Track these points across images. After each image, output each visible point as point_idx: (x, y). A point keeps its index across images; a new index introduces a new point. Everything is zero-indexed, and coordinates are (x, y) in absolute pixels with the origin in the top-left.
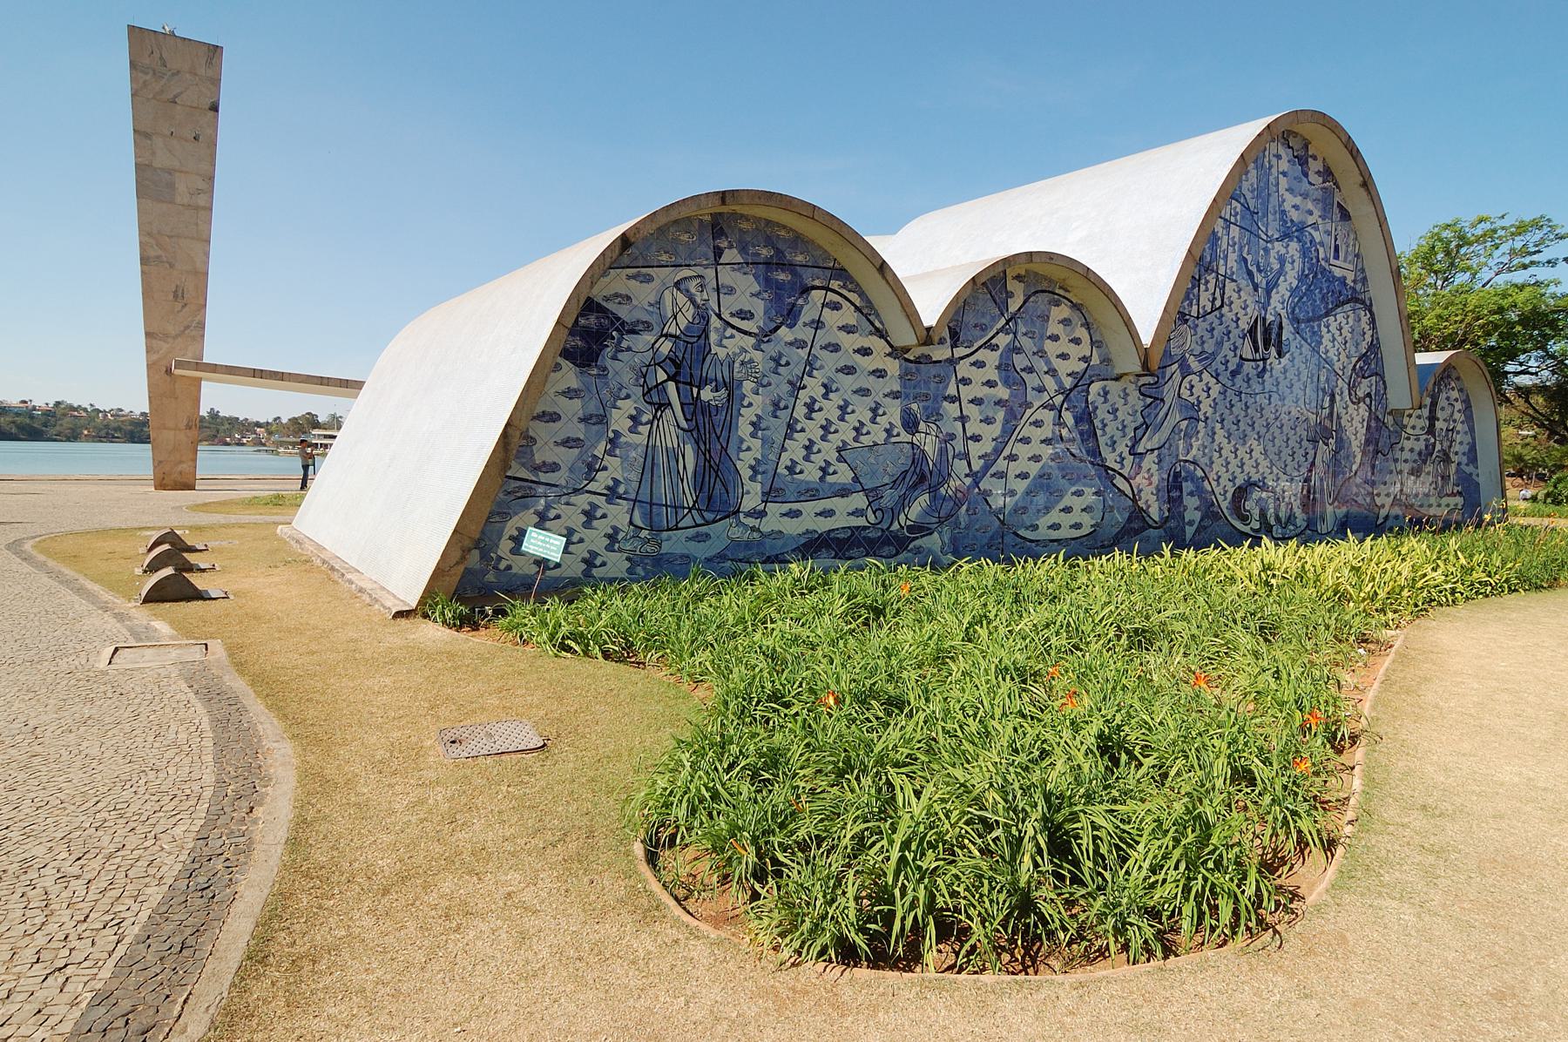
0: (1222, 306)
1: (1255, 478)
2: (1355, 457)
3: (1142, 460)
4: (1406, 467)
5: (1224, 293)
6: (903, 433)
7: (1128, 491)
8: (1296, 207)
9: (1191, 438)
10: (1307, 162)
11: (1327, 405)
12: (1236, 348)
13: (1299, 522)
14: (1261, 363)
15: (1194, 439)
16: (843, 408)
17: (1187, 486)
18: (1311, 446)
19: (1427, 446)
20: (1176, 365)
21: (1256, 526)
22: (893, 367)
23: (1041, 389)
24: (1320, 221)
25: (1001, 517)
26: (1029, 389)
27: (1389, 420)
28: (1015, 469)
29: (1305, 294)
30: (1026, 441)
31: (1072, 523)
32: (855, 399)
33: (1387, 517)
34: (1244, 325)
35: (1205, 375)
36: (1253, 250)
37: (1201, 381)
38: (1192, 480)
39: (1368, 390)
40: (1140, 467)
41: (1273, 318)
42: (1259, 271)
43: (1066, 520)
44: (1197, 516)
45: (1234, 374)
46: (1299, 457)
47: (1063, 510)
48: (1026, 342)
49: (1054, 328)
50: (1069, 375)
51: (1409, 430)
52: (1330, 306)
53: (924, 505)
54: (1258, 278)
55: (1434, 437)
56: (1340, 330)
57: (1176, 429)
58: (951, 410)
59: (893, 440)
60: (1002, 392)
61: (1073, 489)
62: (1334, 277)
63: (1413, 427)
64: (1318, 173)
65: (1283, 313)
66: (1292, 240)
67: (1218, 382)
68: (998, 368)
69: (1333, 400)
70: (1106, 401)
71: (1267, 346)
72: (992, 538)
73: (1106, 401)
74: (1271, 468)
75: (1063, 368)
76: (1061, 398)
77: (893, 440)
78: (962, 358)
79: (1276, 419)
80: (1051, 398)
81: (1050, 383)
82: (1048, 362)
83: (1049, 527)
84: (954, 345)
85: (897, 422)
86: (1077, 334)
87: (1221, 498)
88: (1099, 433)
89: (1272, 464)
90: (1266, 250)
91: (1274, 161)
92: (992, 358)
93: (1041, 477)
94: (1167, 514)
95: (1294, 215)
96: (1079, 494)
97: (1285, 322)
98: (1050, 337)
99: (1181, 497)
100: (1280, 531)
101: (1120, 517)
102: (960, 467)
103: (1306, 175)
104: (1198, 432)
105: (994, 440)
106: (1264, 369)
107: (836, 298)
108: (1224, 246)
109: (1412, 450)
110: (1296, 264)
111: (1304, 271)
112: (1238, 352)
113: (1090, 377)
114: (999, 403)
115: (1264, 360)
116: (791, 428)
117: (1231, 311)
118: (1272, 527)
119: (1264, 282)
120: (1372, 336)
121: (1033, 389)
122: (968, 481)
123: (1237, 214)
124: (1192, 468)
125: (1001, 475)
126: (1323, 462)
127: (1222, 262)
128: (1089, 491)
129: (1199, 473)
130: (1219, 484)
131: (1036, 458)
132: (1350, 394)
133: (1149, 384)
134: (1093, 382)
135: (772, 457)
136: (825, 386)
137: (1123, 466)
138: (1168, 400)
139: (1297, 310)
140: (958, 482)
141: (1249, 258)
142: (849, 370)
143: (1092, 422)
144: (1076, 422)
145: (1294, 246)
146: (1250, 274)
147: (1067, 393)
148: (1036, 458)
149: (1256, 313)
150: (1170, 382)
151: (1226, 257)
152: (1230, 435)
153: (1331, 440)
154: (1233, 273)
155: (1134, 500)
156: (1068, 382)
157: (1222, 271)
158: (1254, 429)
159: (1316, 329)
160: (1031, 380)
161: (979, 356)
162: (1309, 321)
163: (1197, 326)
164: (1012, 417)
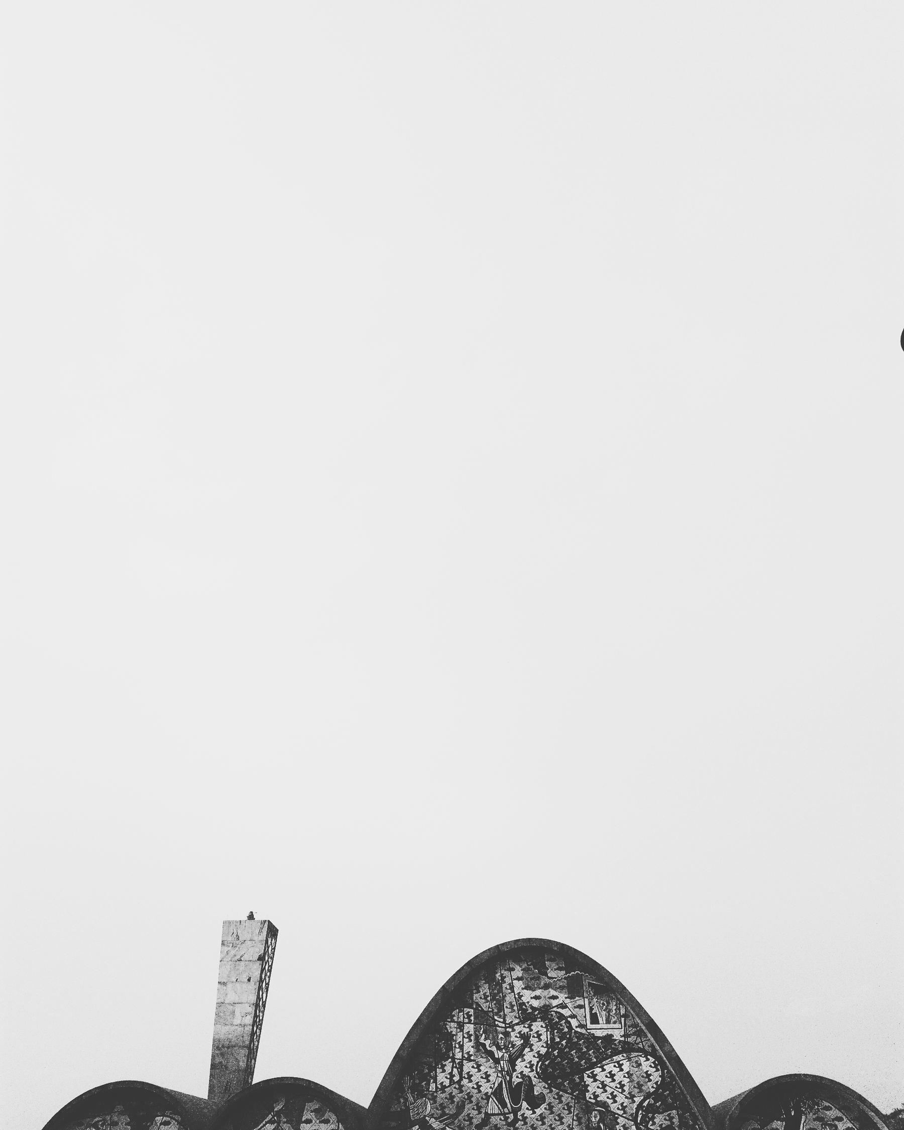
0: (461, 1078)
5: (462, 1070)
24: (567, 1001)
29: (558, 1056)
34: (486, 1088)
42: (499, 1048)
52: (595, 1060)
54: (498, 1054)
56: (612, 1076)
64: (560, 969)
66: (536, 1021)
71: (516, 1100)
86: (326, 1117)
90: (507, 1034)
91: (506, 973)
95: (536, 1003)
97: (535, 1081)
103: (546, 974)
107: (168, 1119)
108: (460, 1039)
110: (543, 1037)
115: (515, 1111)
117: (471, 1081)
119: (506, 1055)
123: (469, 1016)
141: (488, 1043)
145: (538, 1026)
146: (490, 1054)
151: (461, 1047)
157: (459, 1055)
159: (578, 1080)
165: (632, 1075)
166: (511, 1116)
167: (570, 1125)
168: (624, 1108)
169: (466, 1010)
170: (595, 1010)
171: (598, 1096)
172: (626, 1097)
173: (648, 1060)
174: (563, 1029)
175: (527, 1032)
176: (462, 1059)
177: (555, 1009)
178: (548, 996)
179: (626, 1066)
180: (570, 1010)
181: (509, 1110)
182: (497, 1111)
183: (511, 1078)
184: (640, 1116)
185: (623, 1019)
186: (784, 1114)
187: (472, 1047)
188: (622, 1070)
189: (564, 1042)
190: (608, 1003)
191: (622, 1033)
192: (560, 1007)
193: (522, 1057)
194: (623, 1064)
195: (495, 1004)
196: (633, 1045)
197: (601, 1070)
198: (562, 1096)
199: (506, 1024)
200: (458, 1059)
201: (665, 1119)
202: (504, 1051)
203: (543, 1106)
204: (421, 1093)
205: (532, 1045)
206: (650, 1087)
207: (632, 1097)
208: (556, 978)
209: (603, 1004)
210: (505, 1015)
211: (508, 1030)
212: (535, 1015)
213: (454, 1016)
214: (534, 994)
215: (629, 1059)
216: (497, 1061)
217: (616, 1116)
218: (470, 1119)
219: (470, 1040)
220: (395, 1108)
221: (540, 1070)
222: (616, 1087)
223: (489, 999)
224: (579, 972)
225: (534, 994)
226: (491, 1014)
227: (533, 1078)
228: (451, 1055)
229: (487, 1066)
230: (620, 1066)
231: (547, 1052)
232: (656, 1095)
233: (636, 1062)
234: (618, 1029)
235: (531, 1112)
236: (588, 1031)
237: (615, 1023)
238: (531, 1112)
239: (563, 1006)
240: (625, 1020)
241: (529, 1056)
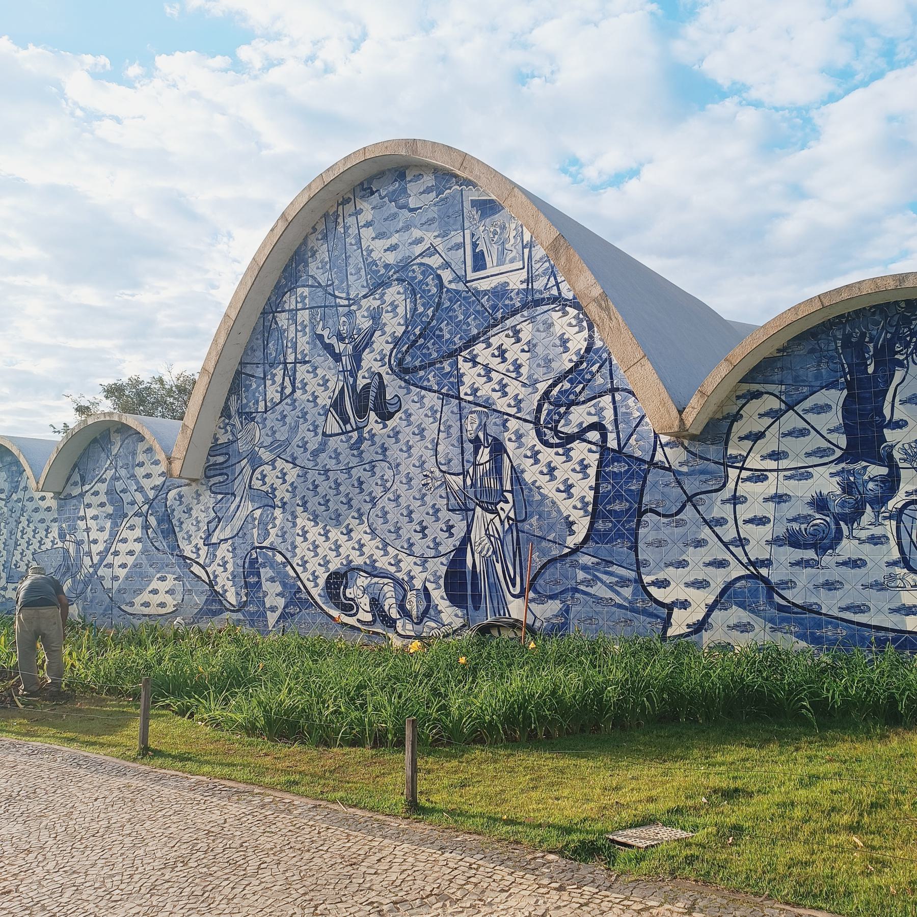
1: (358, 561)
2: (573, 523)
3: (215, 550)
4: (757, 535)
5: (295, 379)
6: (59, 542)
7: (205, 577)
8: (393, 248)
9: (267, 524)
10: (404, 190)
11: (486, 457)
12: (316, 427)
13: (445, 618)
14: (355, 435)
15: (271, 526)
16: (34, 531)
17: (266, 573)
18: (460, 517)
19: (848, 488)
20: (246, 461)
21: (368, 617)
22: (53, 504)
23: (133, 503)
25: (110, 595)
26: (125, 504)
27: (675, 456)
28: (118, 561)
29: (420, 336)
30: (125, 541)
31: (158, 602)
32: (40, 525)
33: (700, 627)
34: (325, 400)
35: (279, 463)
36: (331, 322)
37: (274, 468)
38: (272, 567)
39: (595, 419)
40: (215, 556)
41: (369, 381)
42: (341, 338)
43: (156, 599)
44: (281, 602)
45: (315, 454)
46: (435, 530)
47: (150, 592)
48: (123, 472)
49: (141, 458)
50: (152, 489)
51: (754, 462)
53: (69, 586)
54: (339, 347)
55: (889, 461)
56: (502, 353)
57: (249, 518)
58: (81, 524)
59: (55, 546)
60: (110, 509)
61: (158, 575)
62: (477, 293)
63: (775, 456)
64: (428, 191)
65: (384, 370)
67: (295, 465)
68: (106, 493)
69: (498, 449)
70: (181, 503)
71: (361, 412)
72: (105, 610)
73: (181, 503)
74: (384, 549)
75: (147, 484)
76: (146, 507)
77: (55, 546)
78: (87, 492)
79: (386, 490)
80: (140, 508)
81: (139, 498)
82: (137, 483)
83: (142, 605)
84: (83, 485)
85: (57, 536)
87: (309, 585)
88: (177, 529)
89: (386, 545)
92: (102, 487)
93: (135, 566)
94: (244, 599)
95: (391, 258)
96: (163, 579)
98: (138, 465)
99: (258, 584)
100: (409, 626)
101: (199, 600)
102: (87, 561)
104: (275, 518)
105: (105, 542)
106: (361, 440)
108: (292, 335)
109: (779, 498)
110: (401, 310)
111: (416, 309)
112: (320, 431)
113: (168, 487)
114: (109, 516)
115: (359, 429)
116: (16, 545)
118: (395, 621)
119: (350, 347)
120: (591, 337)
121: (128, 503)
122: (91, 570)
124: (270, 554)
125: (110, 566)
126: (489, 536)
127: (290, 350)
128: (170, 577)
129: (279, 558)
130: (305, 570)
131: (131, 553)
132: (539, 434)
133: (220, 483)
134: (170, 490)
135: (10, 560)
136: (28, 520)
137: (199, 556)
138: (239, 493)
139: (408, 359)
140: (86, 571)
141: (326, 333)
142: (36, 510)
143: (171, 521)
144: (158, 524)
145: (394, 293)
146: (329, 348)
147: (150, 502)
148: (131, 553)
149: (341, 384)
150: (240, 476)
152: (316, 516)
153: (502, 504)
154: (306, 355)
155: (211, 585)
156: (151, 494)
157: (291, 358)
158: (351, 507)
159: (448, 369)
160: (127, 498)
161: (95, 488)
162: (432, 364)
163: (266, 419)
164: (115, 525)
165: (535, 346)
166: (355, 435)
167: (435, 438)
168: (518, 402)
169: (299, 290)
170: (482, 247)
171: (477, 390)
172: (524, 385)
173: (565, 314)
174: (429, 291)
175: (379, 306)
176: (295, 363)
177: (418, 261)
178: (410, 241)
179: (527, 333)
180: (442, 257)
181: (352, 427)
182: (337, 430)
183: (355, 381)
184: (544, 413)
185: (526, 251)
186: (849, 373)
187: (308, 343)
188: (518, 340)
189: (430, 312)
190: (503, 228)
191: (524, 275)
192: (426, 256)
193: (371, 346)
194: (519, 332)
195: (335, 273)
196: (541, 292)
197: (484, 345)
198: (423, 397)
199: (349, 299)
200: (290, 363)
201: (589, 414)
202: (347, 341)
203: (398, 415)
204: (248, 416)
205: (385, 324)
206: (566, 363)
207: (532, 384)
208: (420, 208)
209: (495, 233)
210: (348, 286)
211: (352, 308)
212: (389, 278)
213: (285, 302)
214: (388, 243)
215: (532, 319)
216: (337, 358)
217: (505, 417)
218: (304, 446)
219: (305, 334)
220: (223, 439)
221: (395, 361)
222: (508, 370)
223: (328, 267)
224: (457, 187)
225: (388, 243)
226: (330, 290)
227: (384, 375)
228: (282, 359)
229: (327, 368)
230: (516, 333)
231: (404, 333)
232: (574, 373)
233: (544, 323)
234: (518, 270)
235: (381, 426)
236: (467, 284)
237: (512, 261)
238: (381, 426)
239: (432, 251)
240: (530, 252)
241: (381, 344)
